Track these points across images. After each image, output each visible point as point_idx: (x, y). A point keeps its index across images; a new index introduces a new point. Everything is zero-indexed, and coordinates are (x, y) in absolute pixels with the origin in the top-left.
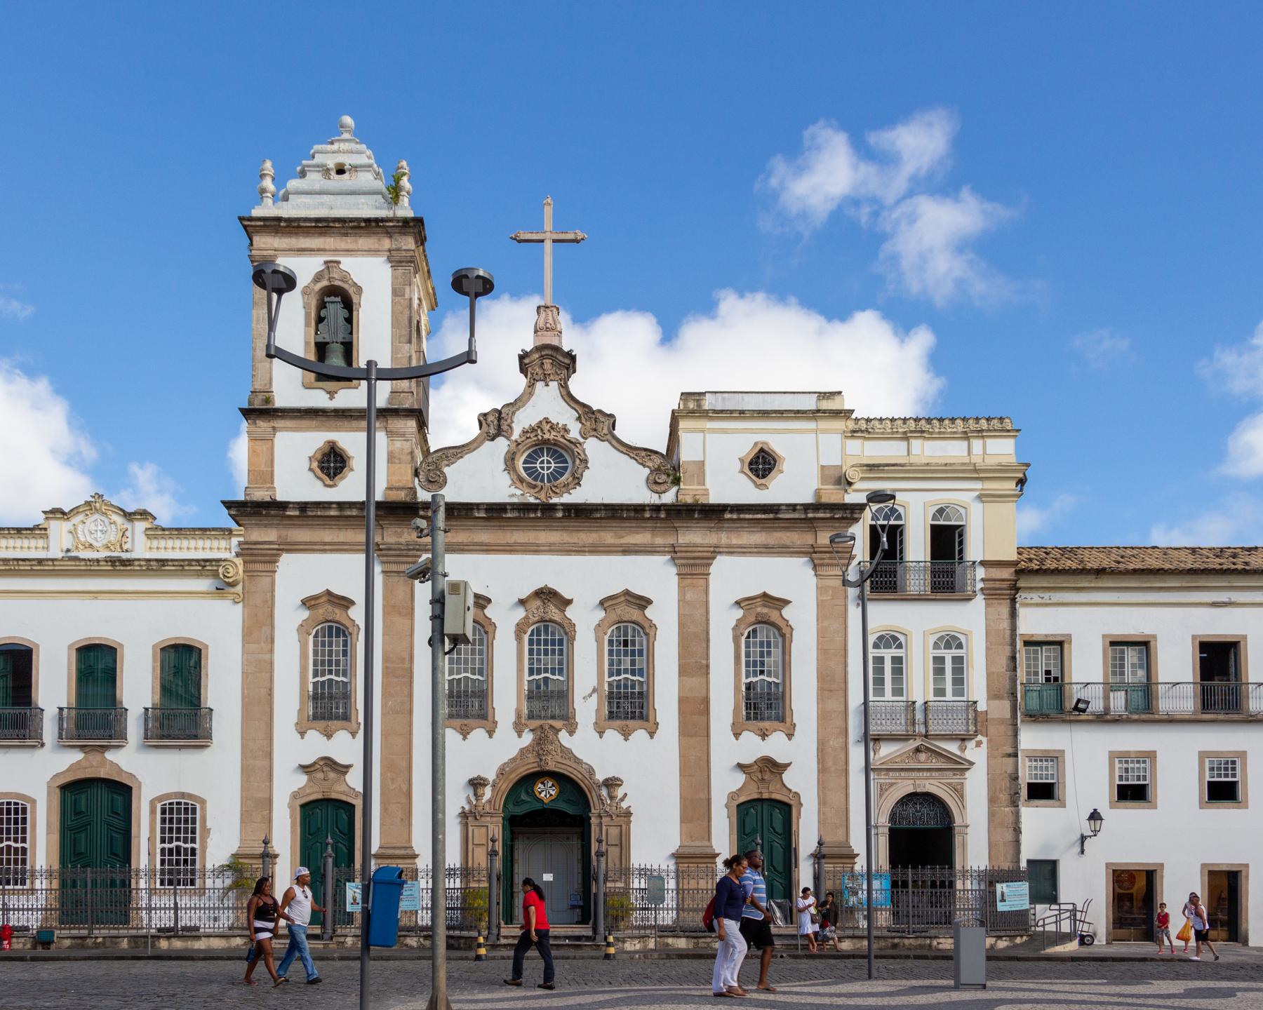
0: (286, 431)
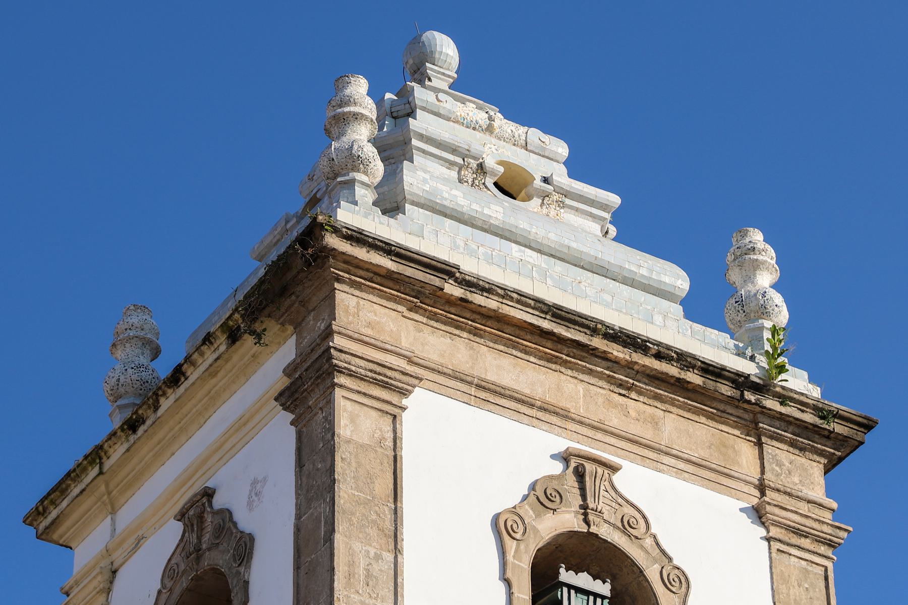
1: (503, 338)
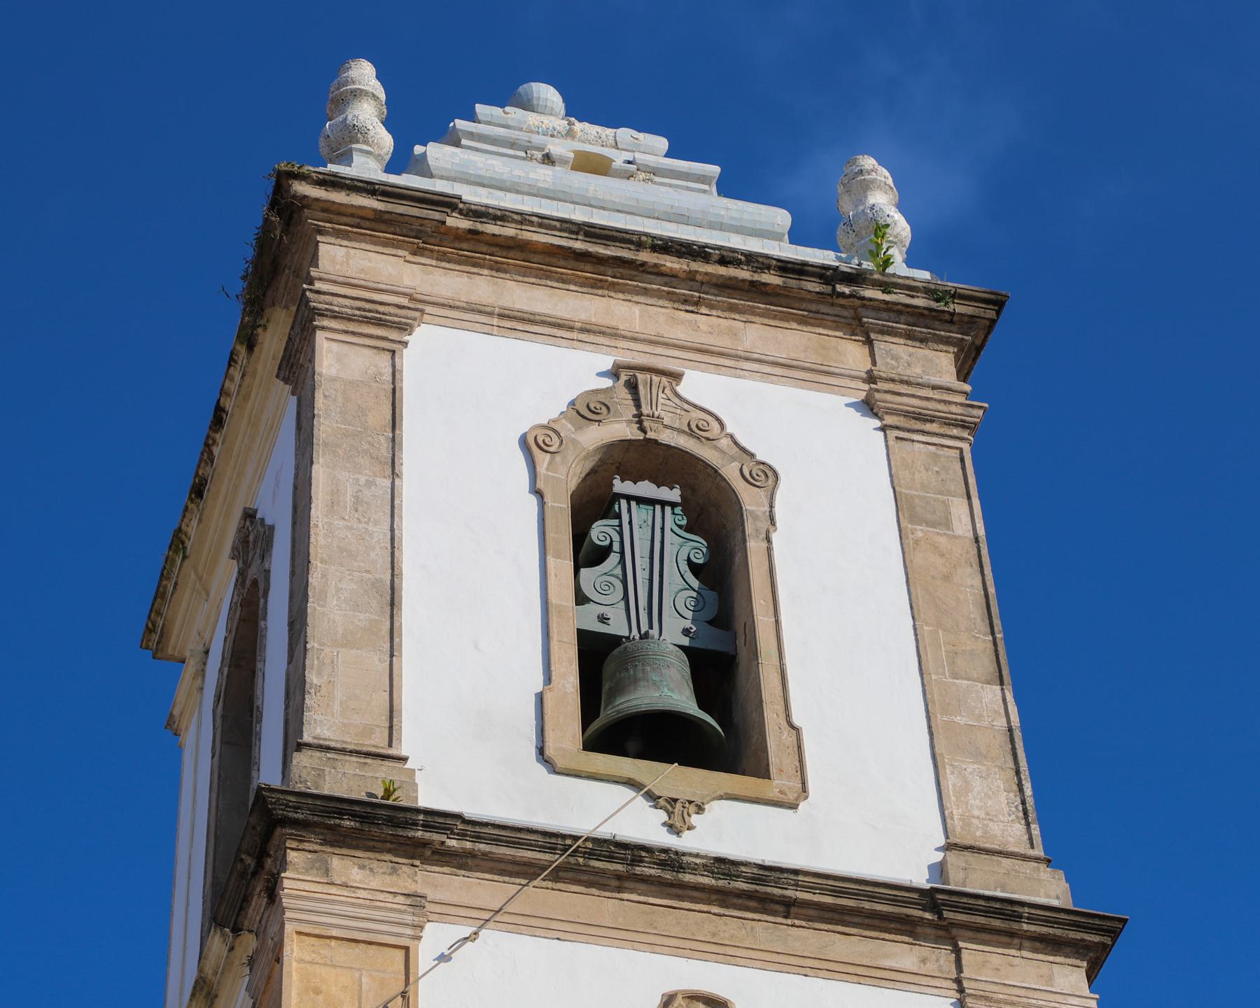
1: (531, 268)
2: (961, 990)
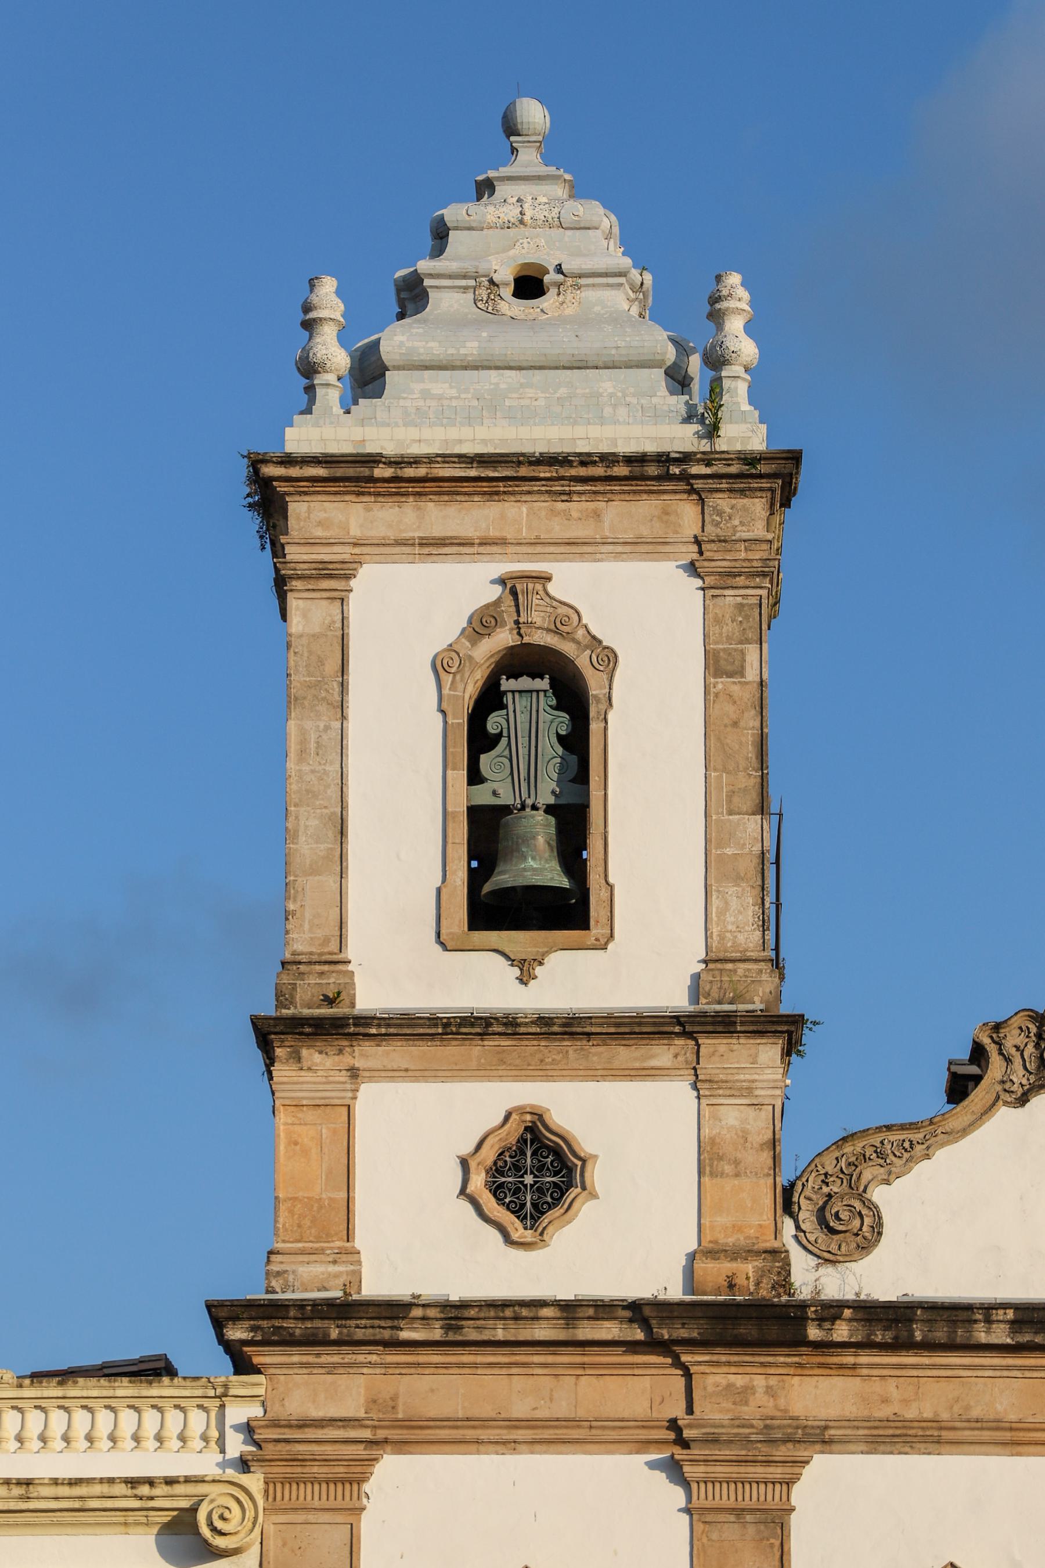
0: (392, 1079)
2: (697, 1076)
